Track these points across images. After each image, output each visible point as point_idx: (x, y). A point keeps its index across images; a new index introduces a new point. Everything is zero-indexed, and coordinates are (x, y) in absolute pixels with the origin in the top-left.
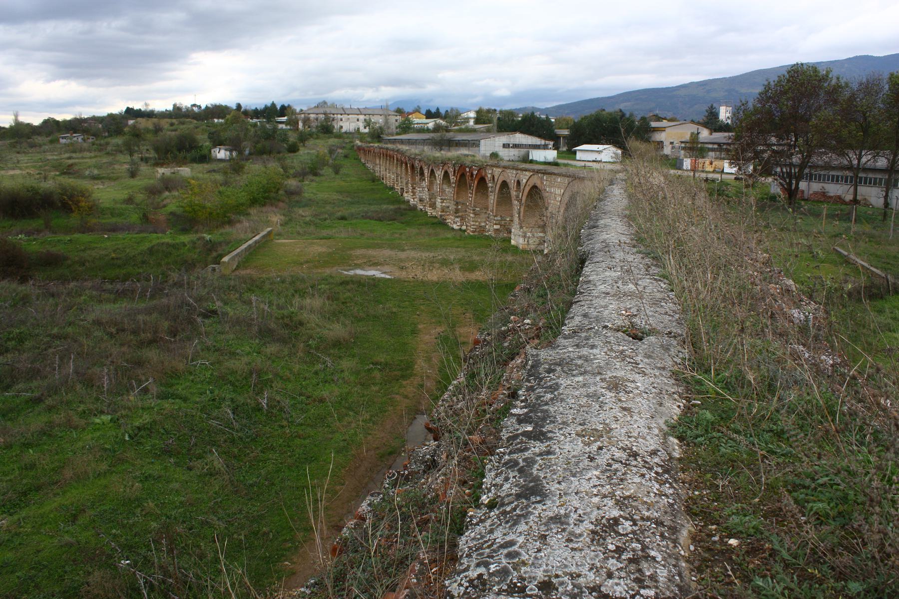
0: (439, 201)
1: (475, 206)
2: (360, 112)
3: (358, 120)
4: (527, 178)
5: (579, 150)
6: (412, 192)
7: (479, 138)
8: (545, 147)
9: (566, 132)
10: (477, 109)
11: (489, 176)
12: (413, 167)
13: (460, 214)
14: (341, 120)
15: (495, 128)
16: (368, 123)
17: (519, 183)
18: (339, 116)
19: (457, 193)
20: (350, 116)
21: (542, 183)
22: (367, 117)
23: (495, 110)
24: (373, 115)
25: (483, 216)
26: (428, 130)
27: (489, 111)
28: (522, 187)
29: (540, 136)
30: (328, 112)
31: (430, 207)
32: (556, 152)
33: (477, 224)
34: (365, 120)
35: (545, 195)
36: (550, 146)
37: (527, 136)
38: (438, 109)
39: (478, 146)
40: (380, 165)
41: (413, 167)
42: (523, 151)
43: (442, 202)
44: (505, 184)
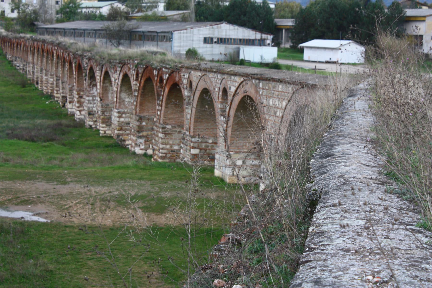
0: (116, 114)
1: (165, 123)
4: (237, 85)
5: (307, 47)
6: (78, 102)
7: (171, 30)
8: (261, 43)
9: (289, 23)
11: (185, 81)
13: (145, 133)
15: (193, 16)
17: (225, 91)
19: (141, 105)
21: (257, 92)
25: (176, 136)
26: (102, 18)
28: (230, 98)
29: (254, 28)
31: (103, 123)
32: (276, 49)
33: (168, 147)
36: (268, 42)
37: (236, 27)
39: (170, 39)
40: (33, 63)
41: (79, 68)
42: (231, 48)
43: (120, 117)
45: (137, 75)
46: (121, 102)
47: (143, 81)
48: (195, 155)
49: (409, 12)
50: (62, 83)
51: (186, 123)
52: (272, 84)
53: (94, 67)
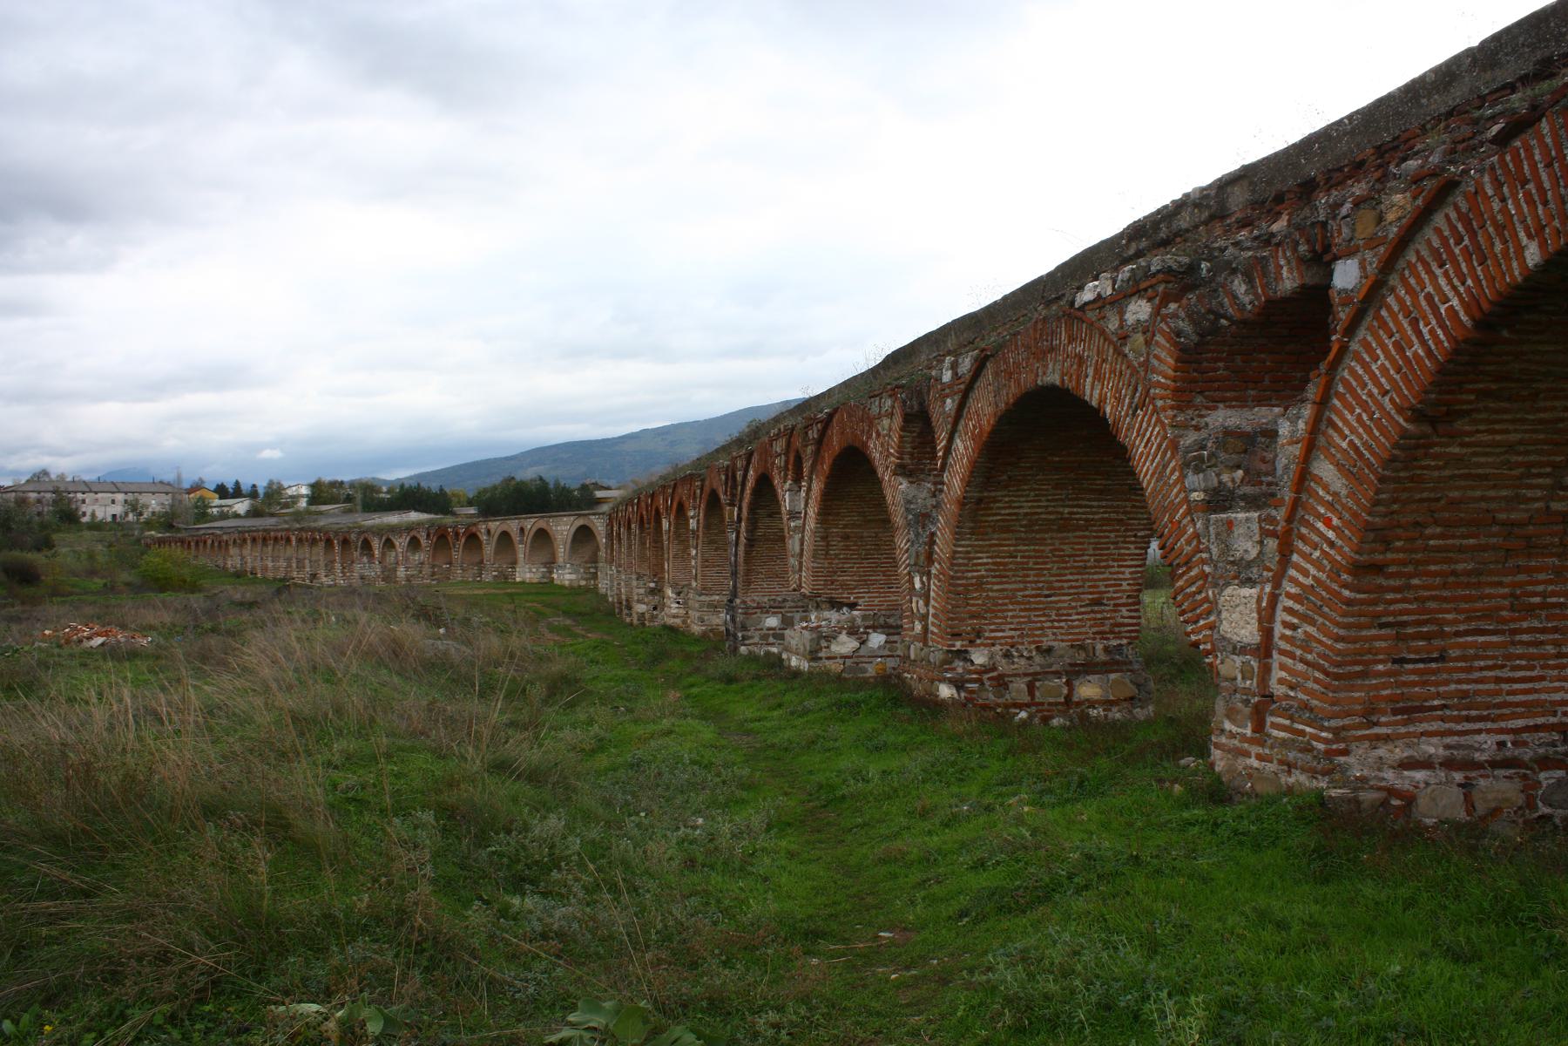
2: (116, 488)
3: (113, 502)
6: (342, 572)
10: (313, 481)
12: (345, 543)
14: (84, 501)
15: (359, 508)
16: (134, 507)
17: (522, 530)
18: (80, 496)
19: (434, 556)
20: (100, 495)
21: (548, 524)
22: (130, 497)
23: (342, 483)
24: (140, 493)
26: (237, 516)
27: (334, 484)
28: (526, 533)
30: (62, 489)
34: (126, 501)
35: (551, 534)
38: (237, 483)
41: (345, 543)
44: (505, 536)
45: (428, 535)
46: (407, 559)
47: (435, 540)
48: (496, 576)
49: (599, 494)
50: (310, 561)
51: (486, 558)
52: (558, 519)
53: (370, 537)
